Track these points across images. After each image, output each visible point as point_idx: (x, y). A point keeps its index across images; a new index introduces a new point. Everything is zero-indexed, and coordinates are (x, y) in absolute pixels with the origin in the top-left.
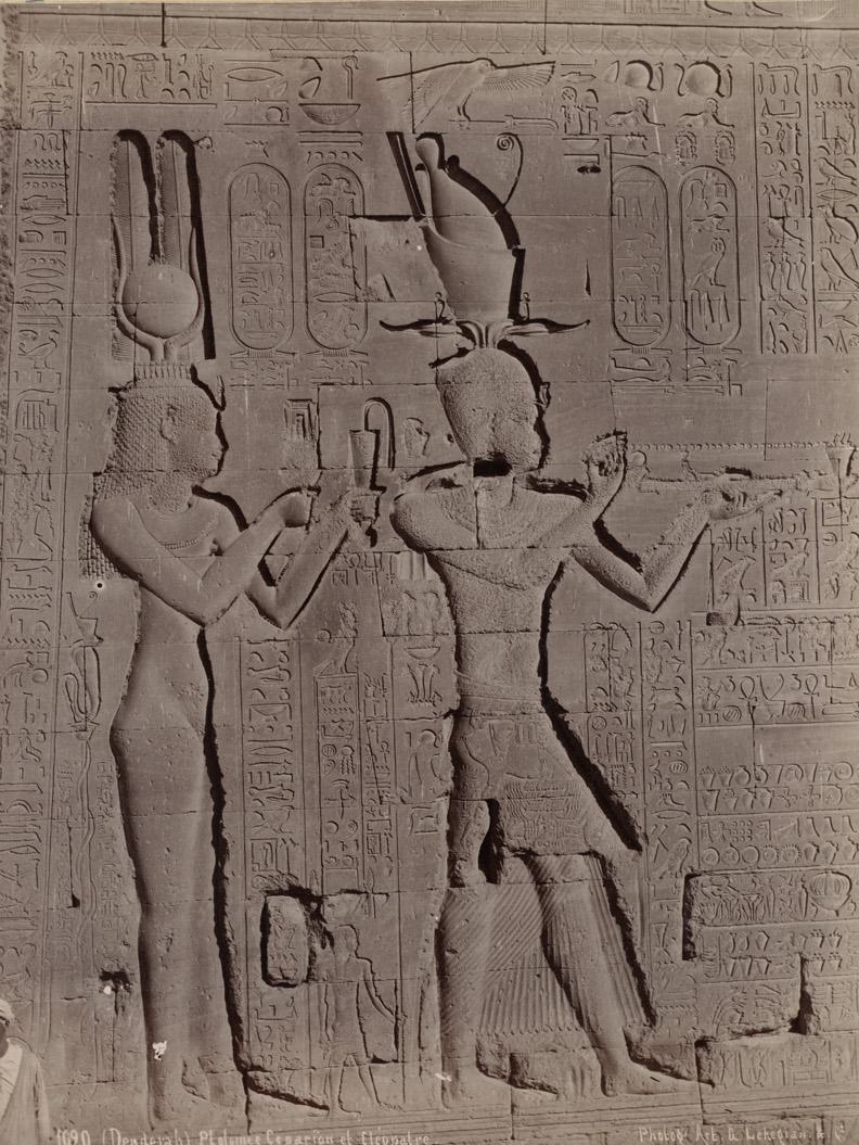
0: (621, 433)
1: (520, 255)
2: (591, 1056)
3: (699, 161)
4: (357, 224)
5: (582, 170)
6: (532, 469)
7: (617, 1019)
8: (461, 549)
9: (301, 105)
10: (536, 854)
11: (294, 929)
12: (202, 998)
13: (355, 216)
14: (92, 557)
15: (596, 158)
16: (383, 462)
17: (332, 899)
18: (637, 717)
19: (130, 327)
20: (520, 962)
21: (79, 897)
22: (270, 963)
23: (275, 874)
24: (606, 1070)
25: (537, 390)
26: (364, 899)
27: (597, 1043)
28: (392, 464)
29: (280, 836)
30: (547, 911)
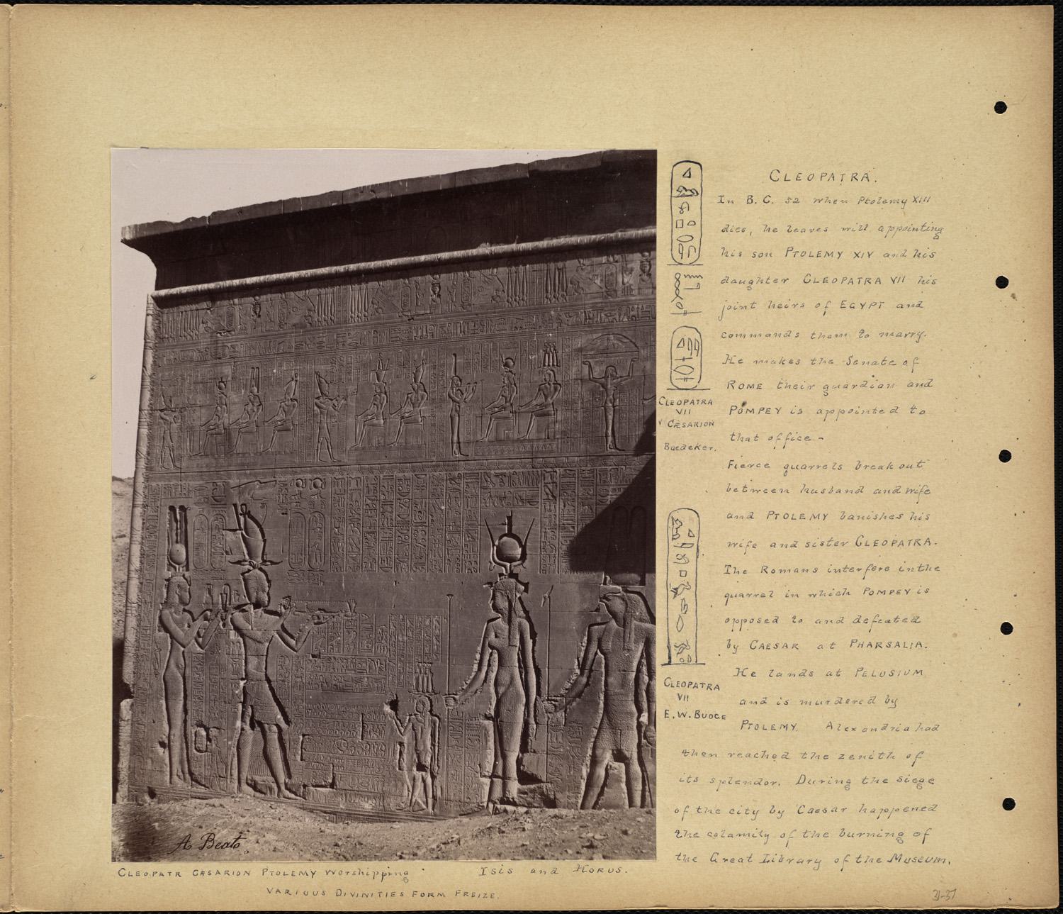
7: (282, 777)
16: (228, 603)
17: (211, 729)
18: (290, 684)
28: (230, 604)
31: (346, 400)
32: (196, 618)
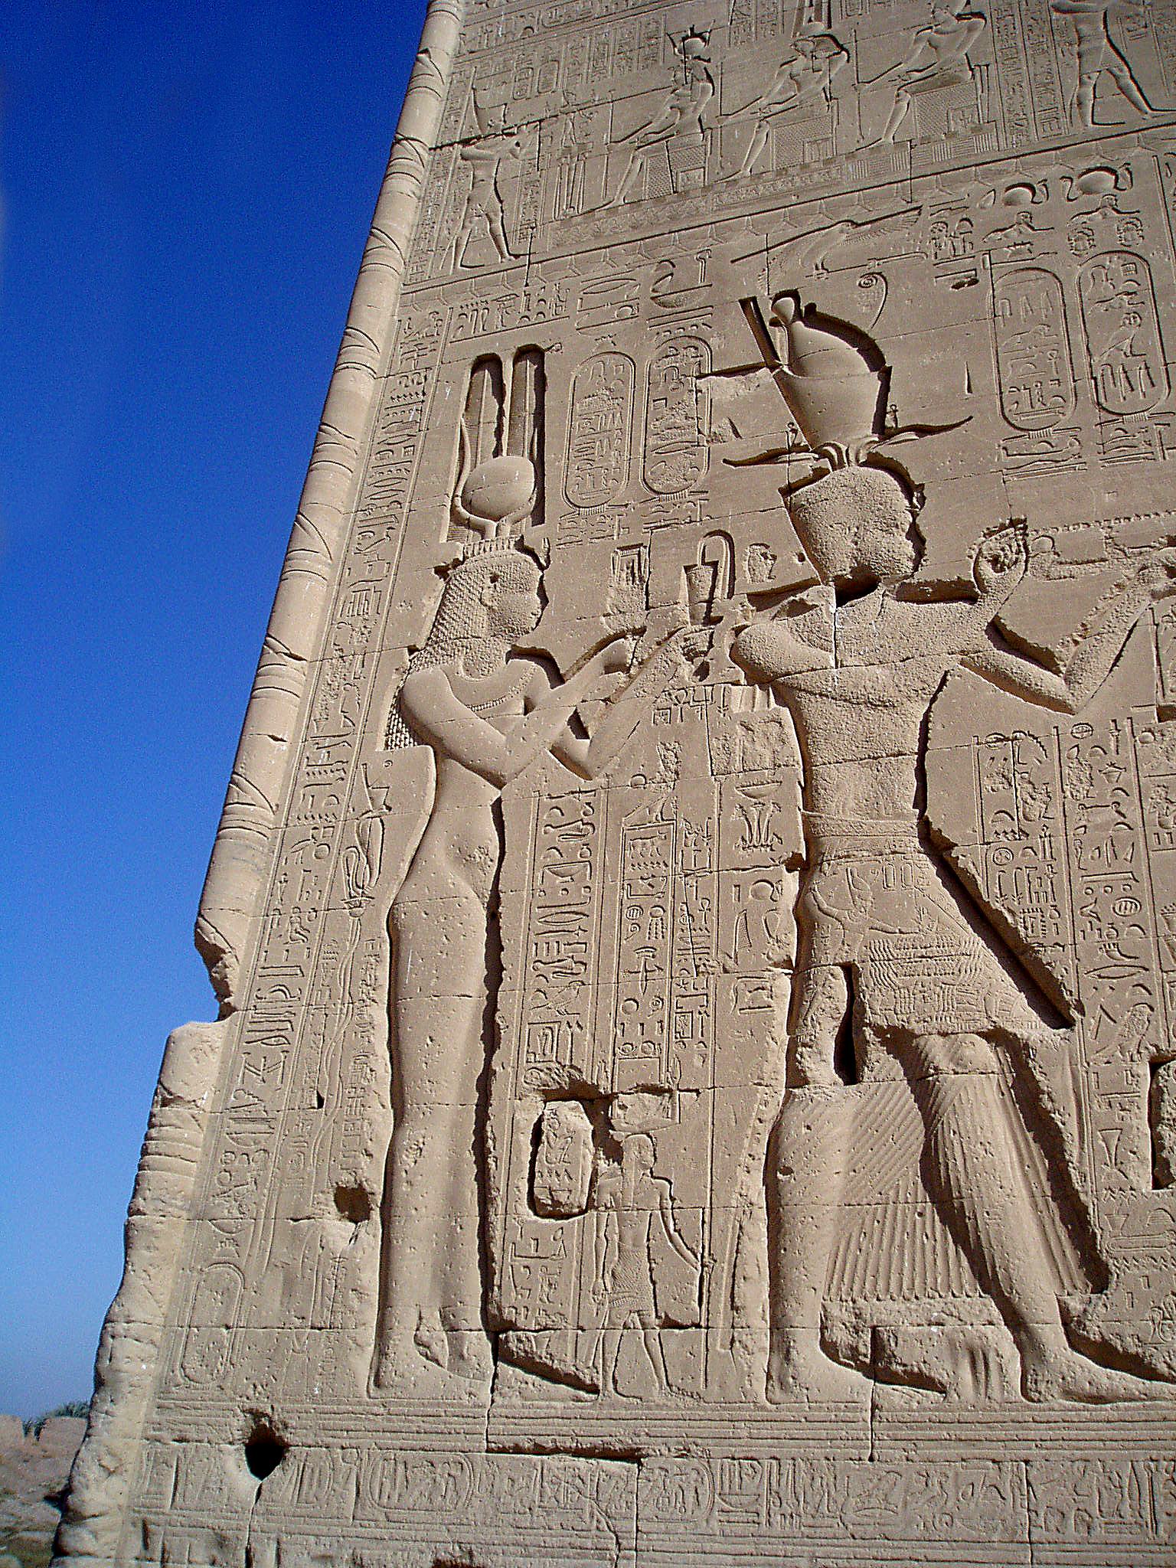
0: (1020, 521)
1: (886, 375)
2: (1002, 1338)
4: (702, 383)
6: (906, 577)
8: (813, 670)
9: (652, 298)
10: (913, 1035)
11: (573, 1135)
12: (452, 1231)
13: (701, 376)
14: (397, 732)
15: (974, 272)
18: (1060, 842)
20: (892, 1193)
21: (324, 1096)
22: (538, 1181)
23: (554, 1065)
24: (1028, 1361)
25: (910, 497)
26: (667, 1098)
27: (1015, 1320)
29: (564, 1019)
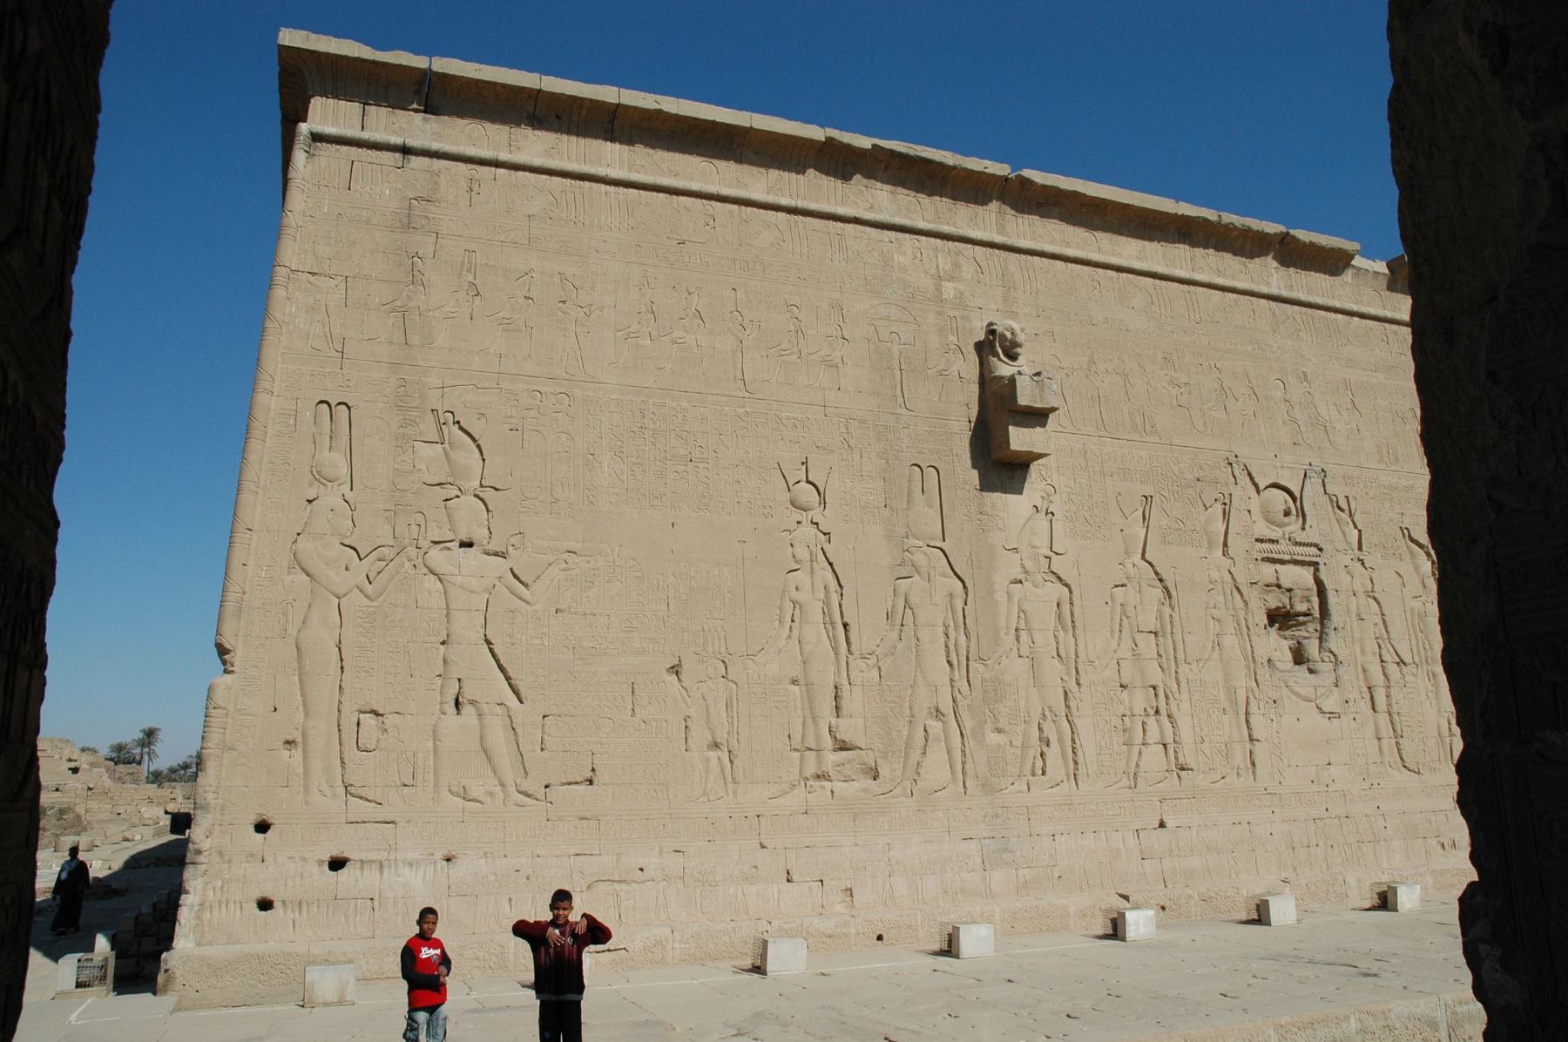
3: (560, 430)
5: (511, 430)
7: (510, 775)
19: (318, 477)
27: (502, 785)
30: (482, 727)
31: (601, 311)
32: (362, 557)
